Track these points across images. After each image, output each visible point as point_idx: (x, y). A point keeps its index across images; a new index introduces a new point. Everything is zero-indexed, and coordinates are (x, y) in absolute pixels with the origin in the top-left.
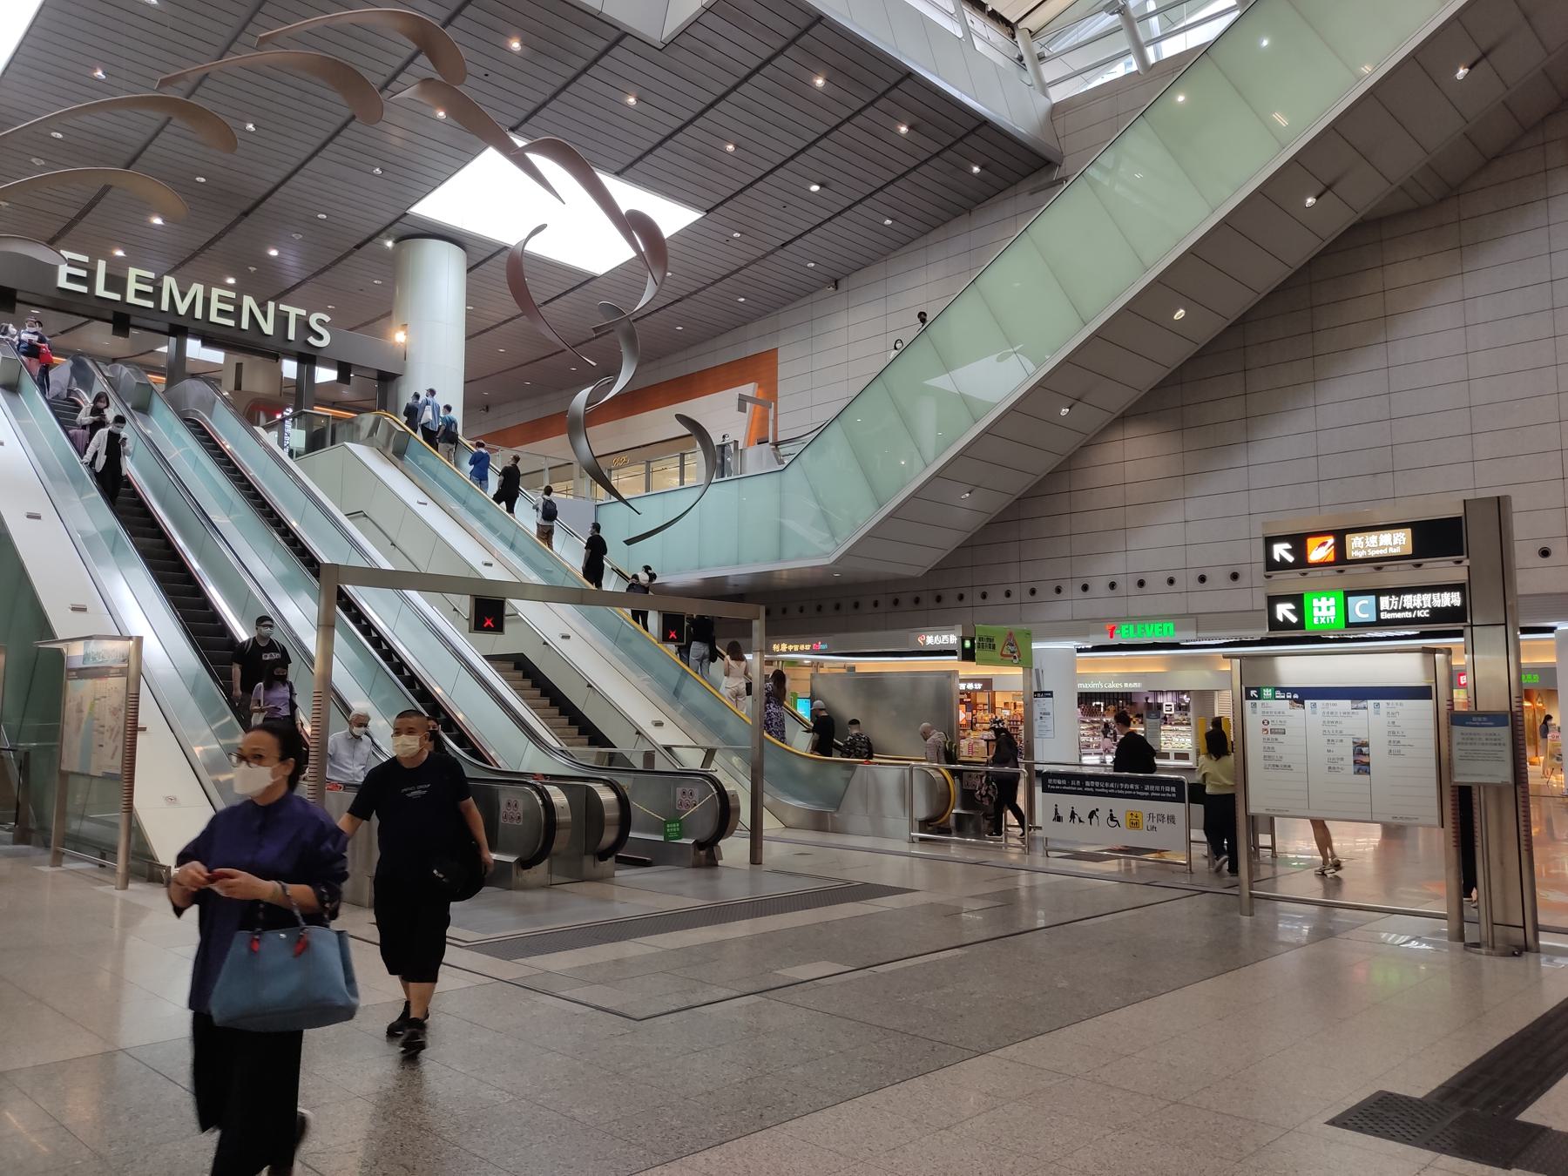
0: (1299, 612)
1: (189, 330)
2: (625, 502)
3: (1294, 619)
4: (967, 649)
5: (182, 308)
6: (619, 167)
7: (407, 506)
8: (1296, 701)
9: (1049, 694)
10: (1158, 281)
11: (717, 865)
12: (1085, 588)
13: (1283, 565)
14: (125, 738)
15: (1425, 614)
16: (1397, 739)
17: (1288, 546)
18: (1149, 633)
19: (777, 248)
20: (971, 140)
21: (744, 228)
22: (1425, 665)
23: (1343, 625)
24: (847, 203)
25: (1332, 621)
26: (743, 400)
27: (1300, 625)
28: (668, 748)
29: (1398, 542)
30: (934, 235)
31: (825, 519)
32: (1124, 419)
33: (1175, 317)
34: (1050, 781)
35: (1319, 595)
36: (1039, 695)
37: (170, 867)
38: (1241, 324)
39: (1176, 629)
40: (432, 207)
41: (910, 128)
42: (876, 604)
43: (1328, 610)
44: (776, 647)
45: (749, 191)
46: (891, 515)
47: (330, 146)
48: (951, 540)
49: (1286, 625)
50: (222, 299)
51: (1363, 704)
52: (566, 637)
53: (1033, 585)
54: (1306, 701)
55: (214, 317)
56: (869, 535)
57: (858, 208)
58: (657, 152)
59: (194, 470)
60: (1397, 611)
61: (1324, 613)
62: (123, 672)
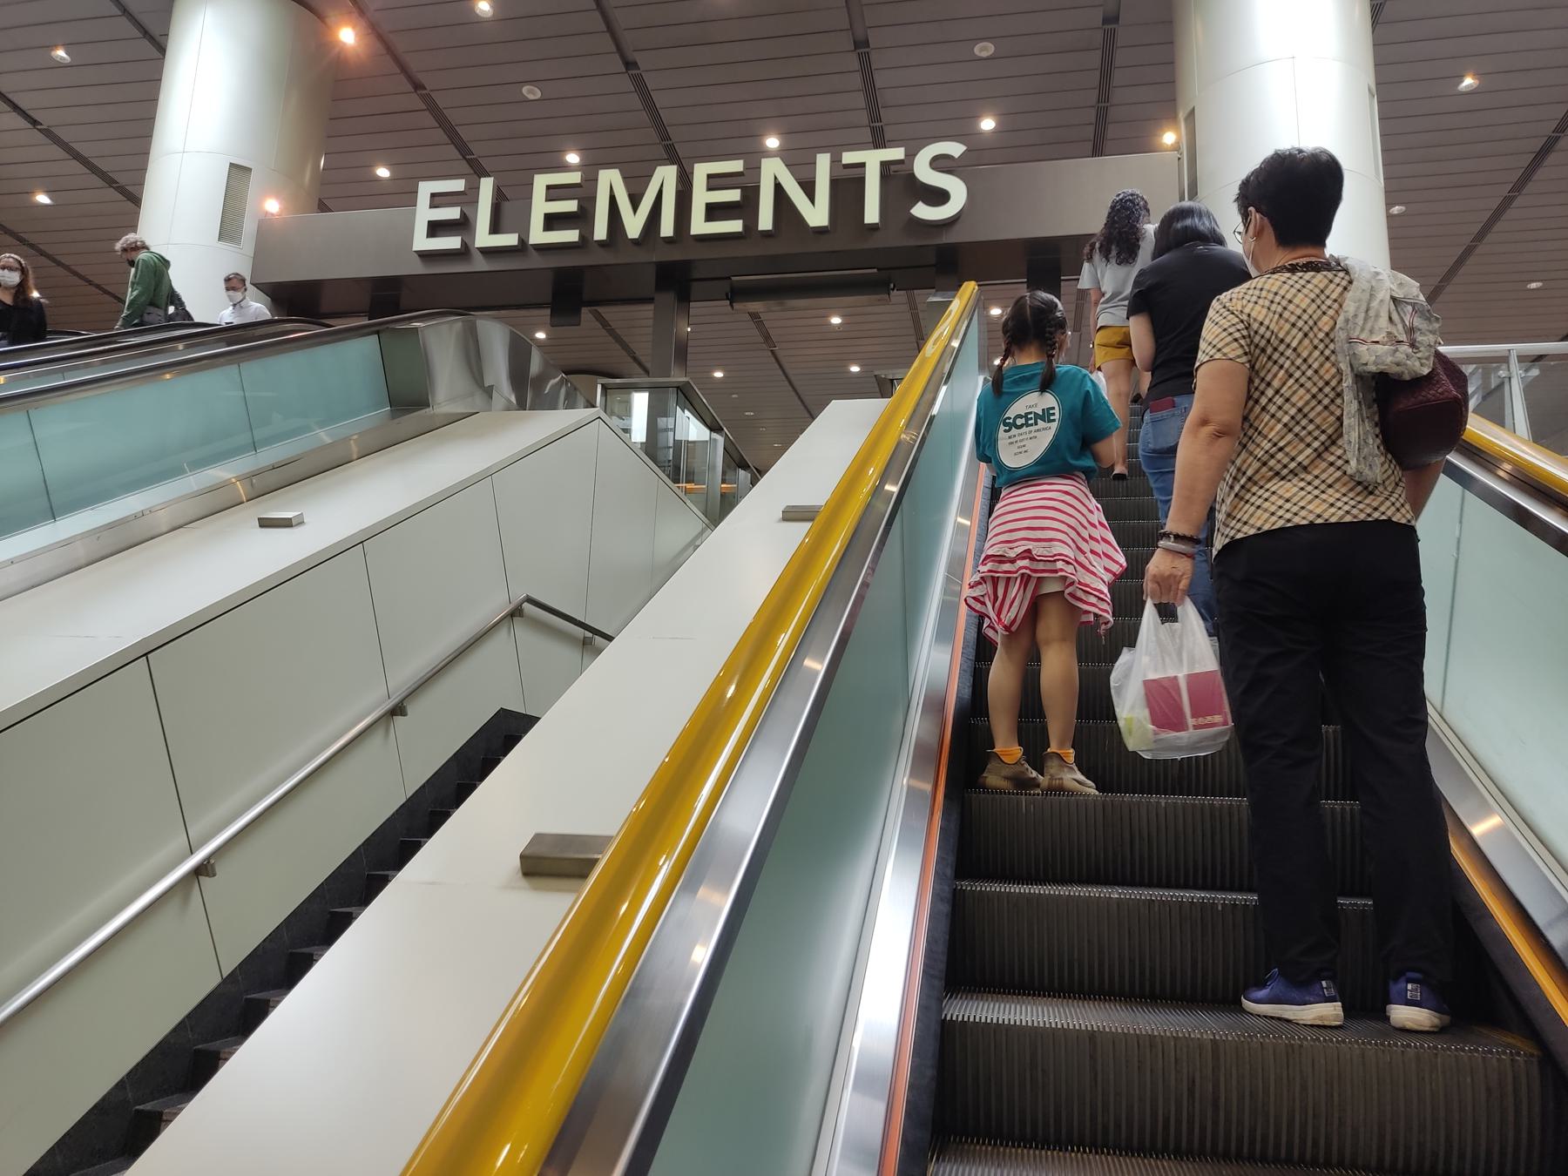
5: (634, 225)
55: (699, 225)
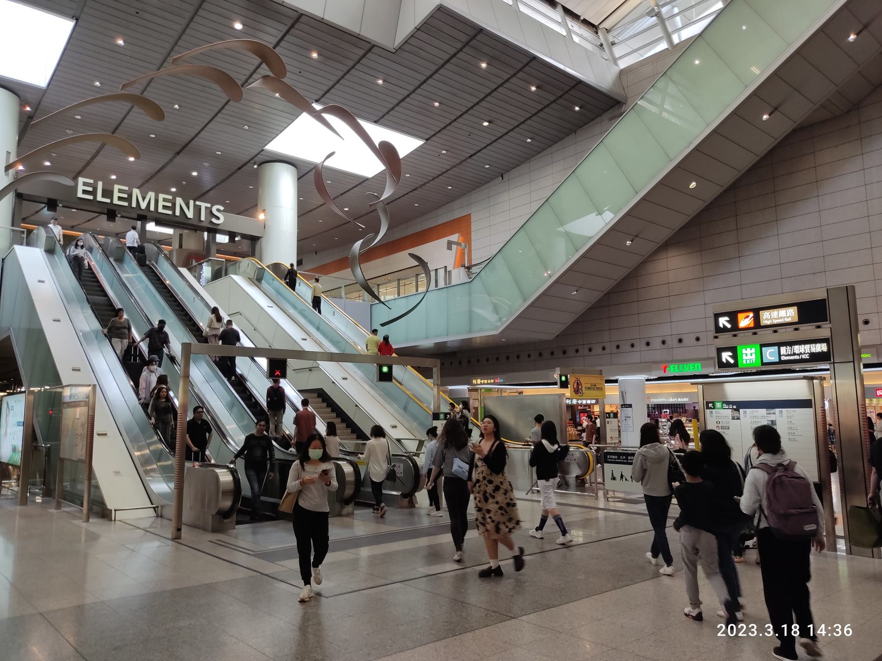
0: (735, 356)
1: (148, 217)
2: (383, 303)
3: (732, 361)
4: (563, 381)
5: (143, 205)
6: (376, 119)
7: (262, 308)
8: (735, 410)
9: (630, 406)
10: (678, 166)
11: (415, 507)
12: (648, 344)
13: (725, 329)
14: (87, 439)
15: (806, 357)
16: (793, 431)
17: (727, 319)
18: (687, 369)
19: (467, 158)
20: (573, 92)
21: (447, 148)
22: (809, 386)
23: (760, 364)
24: (505, 131)
25: (754, 362)
26: (450, 245)
27: (736, 365)
28: (399, 440)
29: (790, 314)
30: (555, 146)
31: (496, 309)
32: (666, 245)
33: (691, 187)
34: (608, 456)
35: (751, 346)
36: (624, 406)
37: (111, 510)
38: (733, 187)
39: (702, 367)
40: (277, 145)
41: (537, 87)
42: (529, 356)
43: (751, 355)
44: (474, 382)
45: (449, 128)
46: (531, 305)
47: (219, 115)
48: (568, 319)
49: (727, 365)
50: (165, 200)
51: (773, 411)
52: (345, 379)
53: (618, 343)
54: (740, 410)
55: (160, 210)
56: (519, 317)
57: (511, 134)
58: (396, 109)
59: (145, 292)
60: (791, 355)
61: (749, 357)
62: (87, 404)
